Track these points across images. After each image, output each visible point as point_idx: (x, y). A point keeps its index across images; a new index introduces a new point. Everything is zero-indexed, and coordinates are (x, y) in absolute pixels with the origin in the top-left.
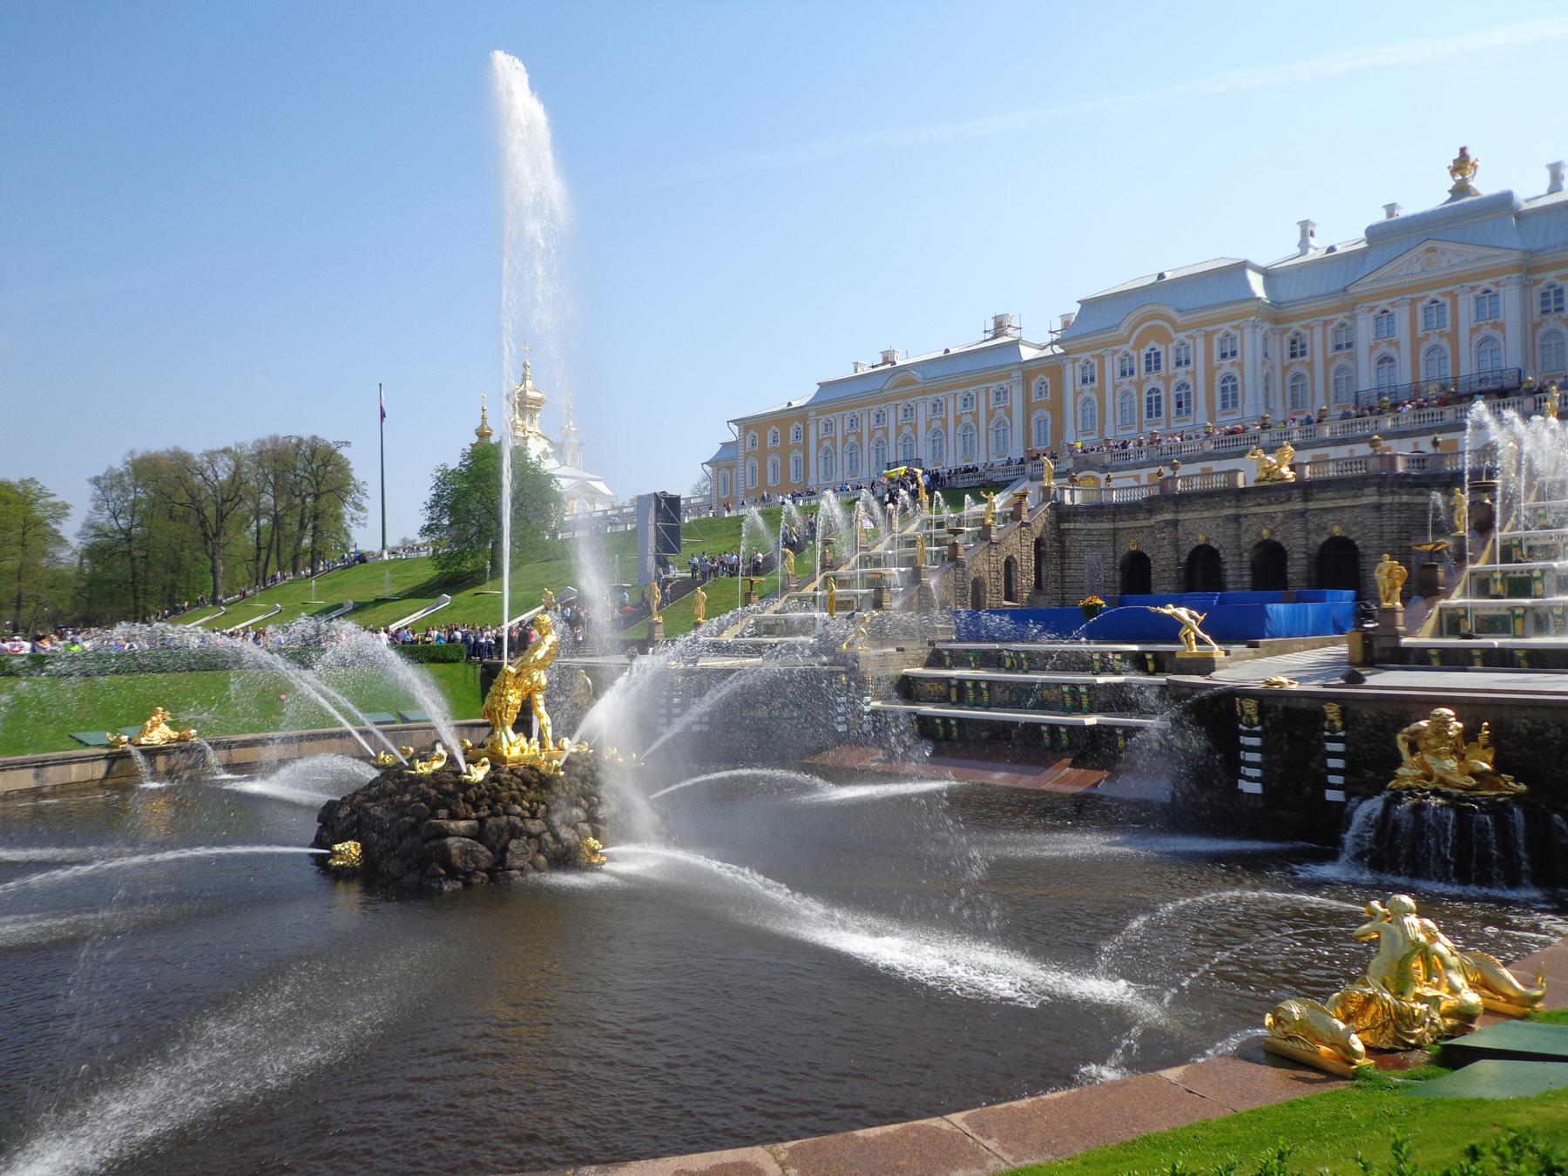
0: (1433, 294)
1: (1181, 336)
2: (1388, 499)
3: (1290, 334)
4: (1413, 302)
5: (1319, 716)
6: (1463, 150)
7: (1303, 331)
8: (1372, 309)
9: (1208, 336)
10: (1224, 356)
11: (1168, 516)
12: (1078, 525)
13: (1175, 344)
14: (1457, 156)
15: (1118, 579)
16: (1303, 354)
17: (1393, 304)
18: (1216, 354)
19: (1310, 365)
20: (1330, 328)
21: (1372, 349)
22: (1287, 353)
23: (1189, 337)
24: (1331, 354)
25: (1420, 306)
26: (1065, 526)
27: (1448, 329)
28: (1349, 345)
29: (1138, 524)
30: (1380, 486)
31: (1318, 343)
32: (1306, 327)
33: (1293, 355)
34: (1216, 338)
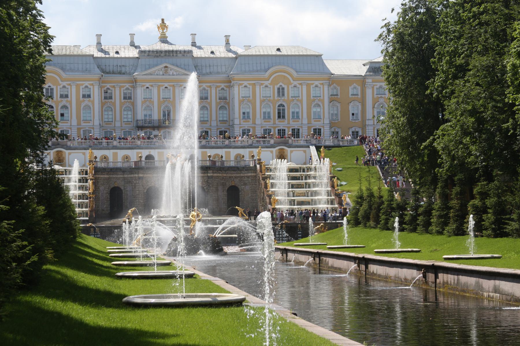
0: (166, 85)
1: (64, 83)
2: (215, 175)
3: (105, 89)
4: (159, 87)
5: (297, 227)
6: (163, 20)
7: (111, 89)
8: (143, 86)
9: (78, 86)
10: (84, 96)
11: (141, 175)
12: (100, 176)
13: (61, 86)
14: (161, 22)
15: (109, 197)
16: (111, 98)
17: (152, 86)
18: (81, 96)
19: (115, 103)
20: (122, 89)
21: (143, 103)
22: (103, 98)
23: (70, 85)
24: (123, 101)
25: (161, 88)
26: (97, 176)
27: (171, 100)
28: (130, 98)
29: (119, 176)
30: (213, 170)
31: (117, 95)
32: (114, 87)
33: (106, 98)
34: (81, 87)
